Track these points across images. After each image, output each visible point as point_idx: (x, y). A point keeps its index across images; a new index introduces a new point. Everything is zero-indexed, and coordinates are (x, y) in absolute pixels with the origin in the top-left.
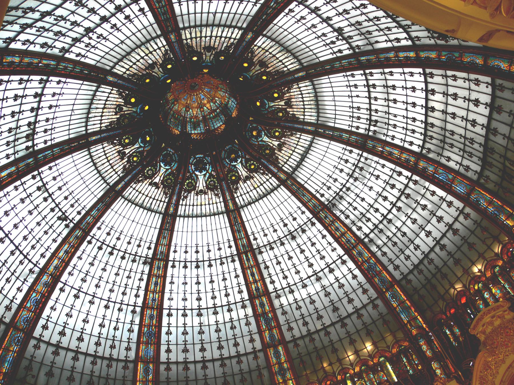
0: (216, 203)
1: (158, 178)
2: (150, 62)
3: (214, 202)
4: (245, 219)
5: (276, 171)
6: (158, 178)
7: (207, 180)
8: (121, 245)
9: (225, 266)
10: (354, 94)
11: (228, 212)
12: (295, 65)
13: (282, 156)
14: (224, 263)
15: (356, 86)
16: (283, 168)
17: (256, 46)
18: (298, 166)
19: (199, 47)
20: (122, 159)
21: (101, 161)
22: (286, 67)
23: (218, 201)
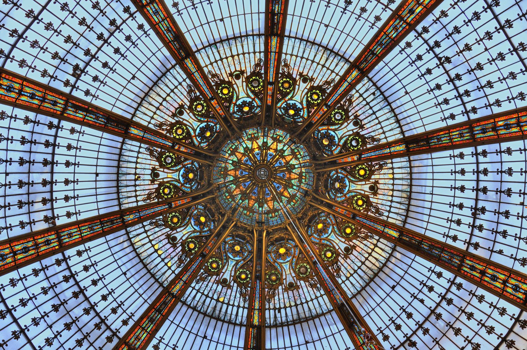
0: (170, 268)
1: (165, 175)
2: (310, 75)
3: (169, 264)
4: (171, 318)
5: (257, 307)
6: (165, 175)
7: (192, 238)
8: (61, 173)
9: (97, 332)
10: (421, 296)
11: (167, 291)
12: (399, 218)
13: (282, 297)
14: (99, 328)
15: (431, 289)
16: (267, 312)
17: (392, 163)
18: (282, 325)
19: (353, 111)
20: (174, 115)
21: (163, 90)
22: (389, 212)
23: (173, 268)
